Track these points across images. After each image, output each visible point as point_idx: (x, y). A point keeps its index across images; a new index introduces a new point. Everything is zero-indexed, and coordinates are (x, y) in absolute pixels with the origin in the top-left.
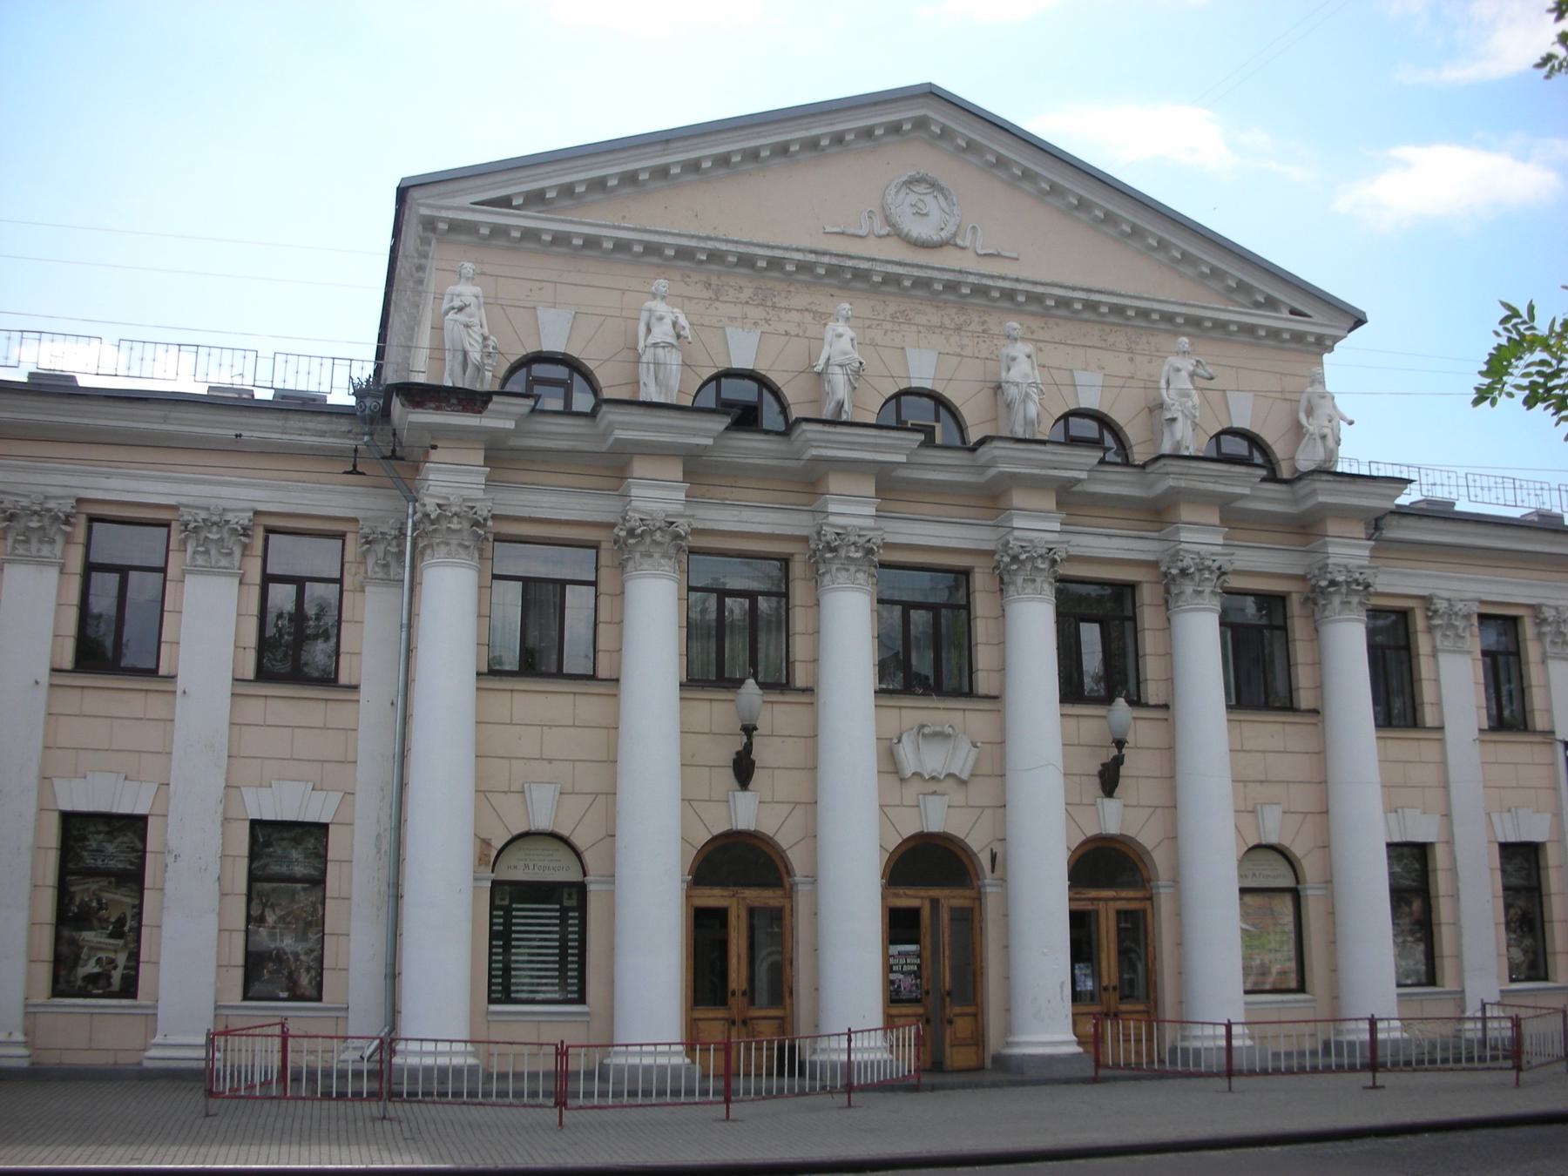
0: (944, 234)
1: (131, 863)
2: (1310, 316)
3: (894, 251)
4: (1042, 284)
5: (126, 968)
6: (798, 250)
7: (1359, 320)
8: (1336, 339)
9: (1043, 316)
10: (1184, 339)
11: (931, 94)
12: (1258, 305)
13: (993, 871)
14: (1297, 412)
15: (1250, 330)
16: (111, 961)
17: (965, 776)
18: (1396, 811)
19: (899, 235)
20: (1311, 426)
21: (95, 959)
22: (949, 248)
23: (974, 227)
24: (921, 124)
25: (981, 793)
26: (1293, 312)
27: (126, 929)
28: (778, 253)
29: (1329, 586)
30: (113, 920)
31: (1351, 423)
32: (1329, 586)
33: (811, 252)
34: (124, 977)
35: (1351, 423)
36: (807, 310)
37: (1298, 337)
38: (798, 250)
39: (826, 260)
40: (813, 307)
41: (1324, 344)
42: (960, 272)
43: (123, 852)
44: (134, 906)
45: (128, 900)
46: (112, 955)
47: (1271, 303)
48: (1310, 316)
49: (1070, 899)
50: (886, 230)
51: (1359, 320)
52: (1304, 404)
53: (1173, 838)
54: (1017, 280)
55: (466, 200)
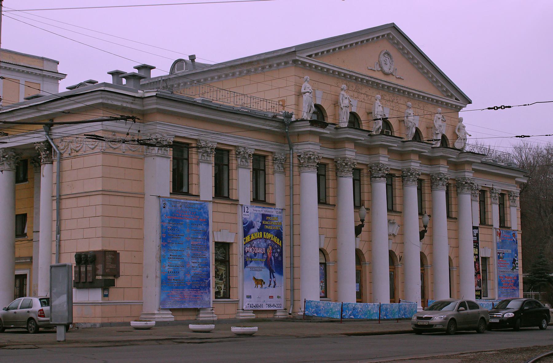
0: (391, 71)
1: (223, 257)
2: (459, 101)
3: (379, 76)
4: (412, 89)
5: (224, 289)
6: (367, 76)
7: (470, 102)
8: (461, 108)
9: (408, 98)
10: (440, 109)
11: (393, 27)
12: (448, 96)
13: (400, 261)
14: (455, 130)
15: (447, 104)
16: (221, 287)
17: (396, 234)
18: (220, 231)
19: (382, 71)
20: (460, 135)
21: (217, 287)
22: (391, 75)
23: (396, 69)
24: (388, 35)
25: (398, 239)
26: (456, 99)
27: (223, 277)
28: (364, 77)
29: (465, 184)
30: (220, 275)
31: (470, 136)
32: (465, 184)
33: (370, 77)
34: (224, 292)
35: (470, 136)
36: (365, 94)
37: (456, 106)
38: (367, 76)
39: (373, 80)
40: (366, 93)
41: (458, 109)
42: (397, 85)
43: (221, 254)
44: (225, 270)
45: (223, 268)
46: (220, 286)
47: (451, 96)
48: (459, 101)
49: (390, 269)
50: (380, 69)
51: (470, 102)
52: (457, 127)
53: (370, 251)
54: (407, 88)
55: (304, 55)
